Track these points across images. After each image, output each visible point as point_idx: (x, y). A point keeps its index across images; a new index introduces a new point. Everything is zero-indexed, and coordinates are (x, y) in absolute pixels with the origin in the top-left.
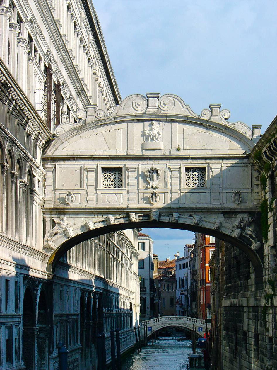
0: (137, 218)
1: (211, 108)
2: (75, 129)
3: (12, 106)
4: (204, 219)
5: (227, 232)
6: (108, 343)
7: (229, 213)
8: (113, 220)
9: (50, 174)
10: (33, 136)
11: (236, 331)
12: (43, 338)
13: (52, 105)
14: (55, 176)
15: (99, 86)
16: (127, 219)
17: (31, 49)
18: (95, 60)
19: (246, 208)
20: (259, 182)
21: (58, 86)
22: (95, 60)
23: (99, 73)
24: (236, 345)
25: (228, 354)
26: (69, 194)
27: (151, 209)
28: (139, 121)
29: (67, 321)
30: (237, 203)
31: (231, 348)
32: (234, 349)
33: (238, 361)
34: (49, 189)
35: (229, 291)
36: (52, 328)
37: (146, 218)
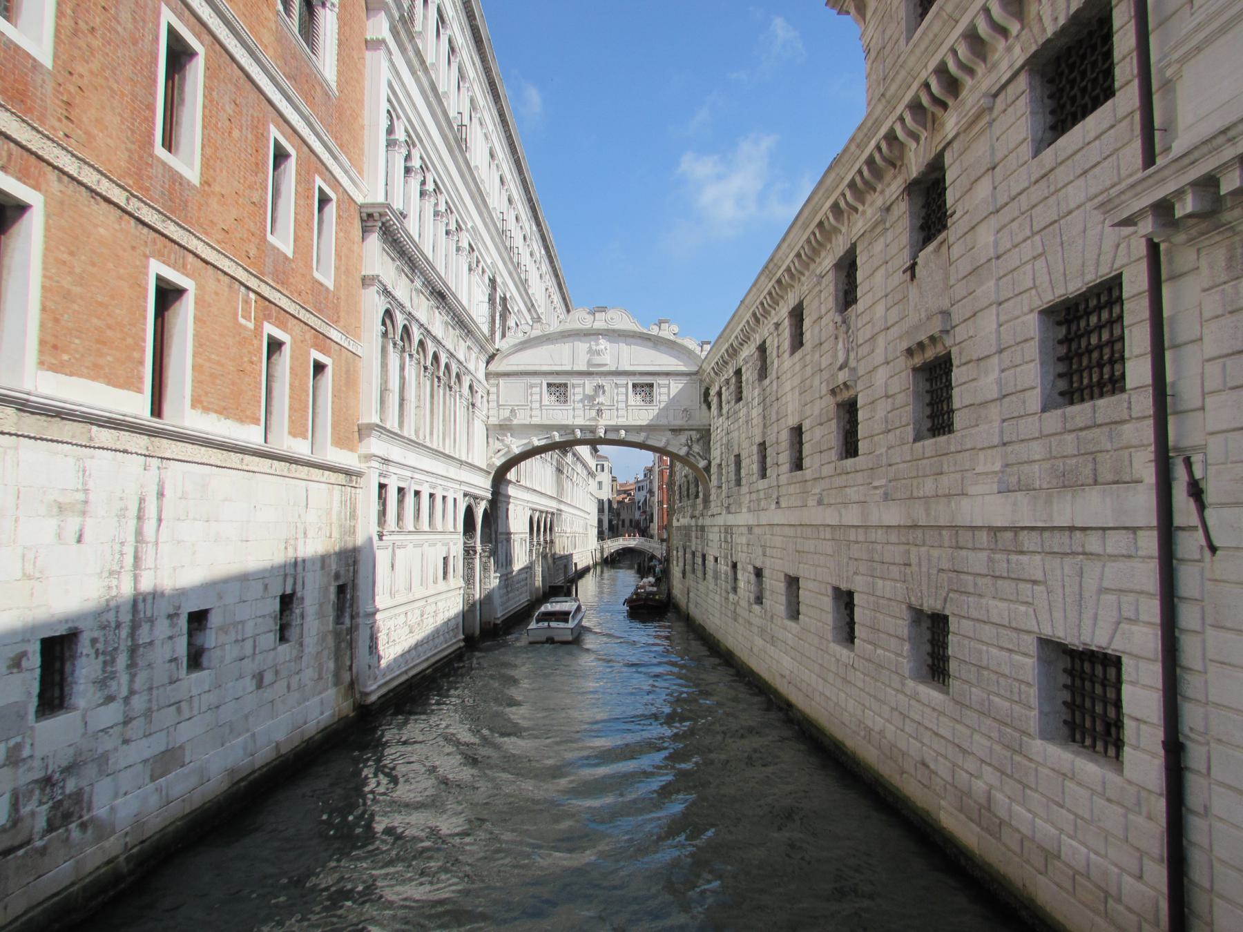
5: (674, 450)
7: (676, 431)
8: (557, 437)
9: (493, 390)
13: (498, 318)
14: (498, 391)
18: (548, 276)
21: (504, 299)
23: (551, 290)
27: (597, 426)
28: (585, 335)
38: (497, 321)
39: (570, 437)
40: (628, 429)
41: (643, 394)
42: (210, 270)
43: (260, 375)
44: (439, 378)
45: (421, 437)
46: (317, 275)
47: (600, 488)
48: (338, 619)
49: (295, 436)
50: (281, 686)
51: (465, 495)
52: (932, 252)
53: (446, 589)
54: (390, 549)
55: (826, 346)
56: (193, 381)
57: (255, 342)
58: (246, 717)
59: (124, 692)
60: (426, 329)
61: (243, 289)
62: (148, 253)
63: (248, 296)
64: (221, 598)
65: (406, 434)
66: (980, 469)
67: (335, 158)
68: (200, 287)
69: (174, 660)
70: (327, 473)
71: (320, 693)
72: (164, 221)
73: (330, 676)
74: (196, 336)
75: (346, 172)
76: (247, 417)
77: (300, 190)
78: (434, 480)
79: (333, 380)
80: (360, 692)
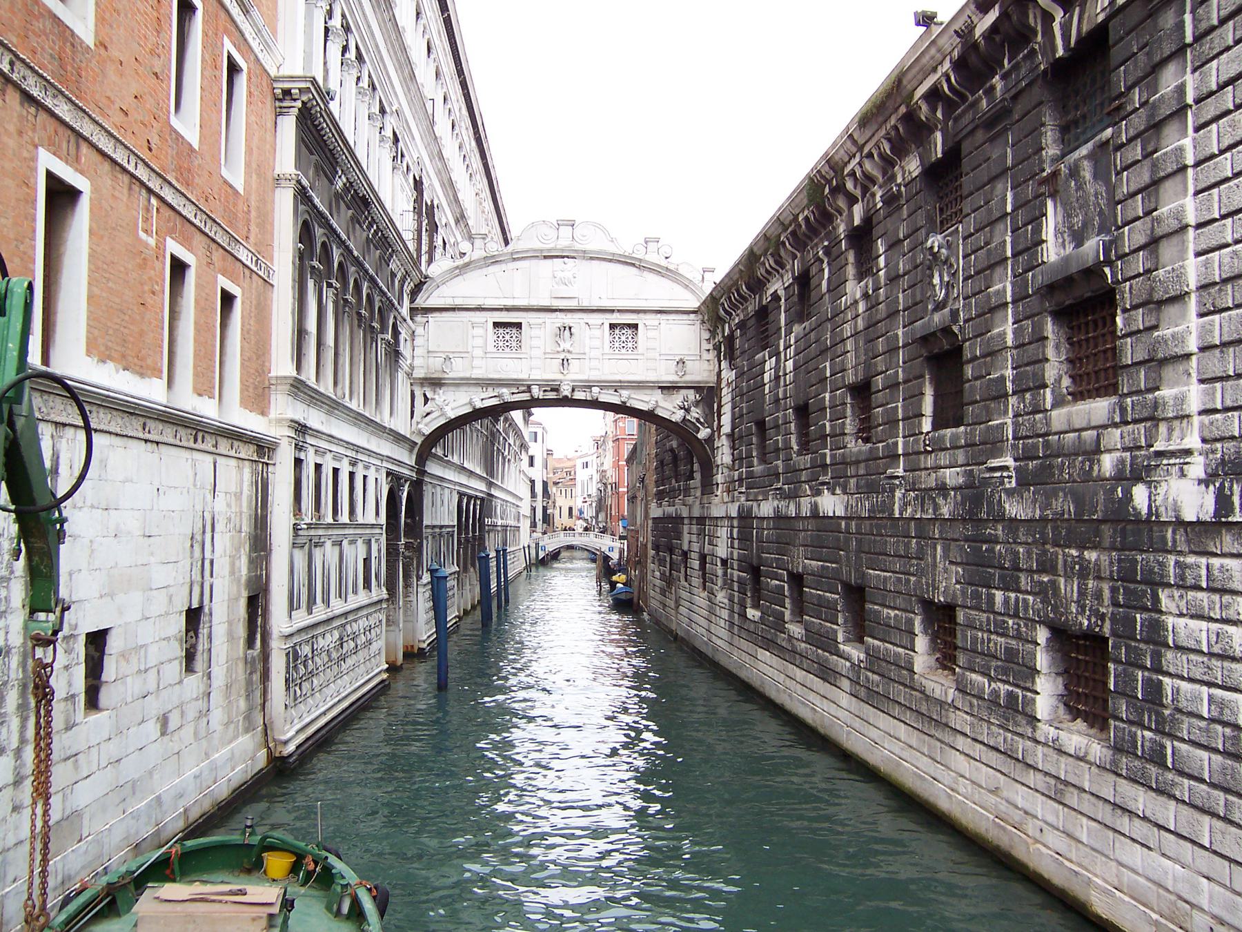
0: (542, 393)
1: (646, 242)
2: (457, 268)
3: (372, 231)
4: (633, 396)
6: (493, 564)
7: (668, 389)
8: (508, 395)
9: (419, 331)
10: (399, 276)
11: (671, 552)
12: (409, 557)
13: (424, 233)
15: (483, 212)
16: (528, 394)
17: (397, 153)
18: (478, 177)
19: (691, 382)
20: (710, 347)
21: (431, 209)
22: (478, 177)
23: (483, 195)
24: (671, 570)
25: (658, 582)
26: (448, 359)
28: (545, 257)
29: (440, 534)
30: (681, 374)
31: (663, 574)
32: (668, 574)
33: (673, 591)
34: (418, 352)
35: (660, 496)
36: (421, 544)
37: (555, 393)
38: (424, 237)
39: (526, 397)
40: (604, 385)
41: (623, 338)
42: (107, 166)
43: (162, 312)
44: (359, 314)
45: (339, 393)
46: (224, 172)
47: (531, 464)
48: (250, 643)
49: (200, 395)
50: (187, 733)
51: (388, 474)
52: (1085, 157)
53: (367, 602)
54: (307, 547)
55: (905, 282)
56: (88, 318)
57: (158, 265)
58: (151, 773)
59: (15, 744)
60: (347, 248)
61: (144, 191)
62: (36, 140)
63: (149, 201)
64: (121, 613)
65: (322, 390)
66: (1159, 446)
67: (246, 12)
68: (95, 189)
69: (71, 698)
70: (236, 444)
71: (231, 742)
72: (55, 97)
73: (241, 718)
74: (93, 256)
75: (258, 32)
76: (148, 367)
77: (207, 57)
78: (353, 454)
79: (243, 317)
80: (274, 740)
